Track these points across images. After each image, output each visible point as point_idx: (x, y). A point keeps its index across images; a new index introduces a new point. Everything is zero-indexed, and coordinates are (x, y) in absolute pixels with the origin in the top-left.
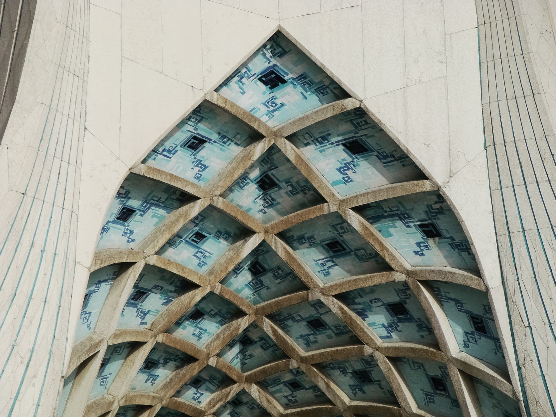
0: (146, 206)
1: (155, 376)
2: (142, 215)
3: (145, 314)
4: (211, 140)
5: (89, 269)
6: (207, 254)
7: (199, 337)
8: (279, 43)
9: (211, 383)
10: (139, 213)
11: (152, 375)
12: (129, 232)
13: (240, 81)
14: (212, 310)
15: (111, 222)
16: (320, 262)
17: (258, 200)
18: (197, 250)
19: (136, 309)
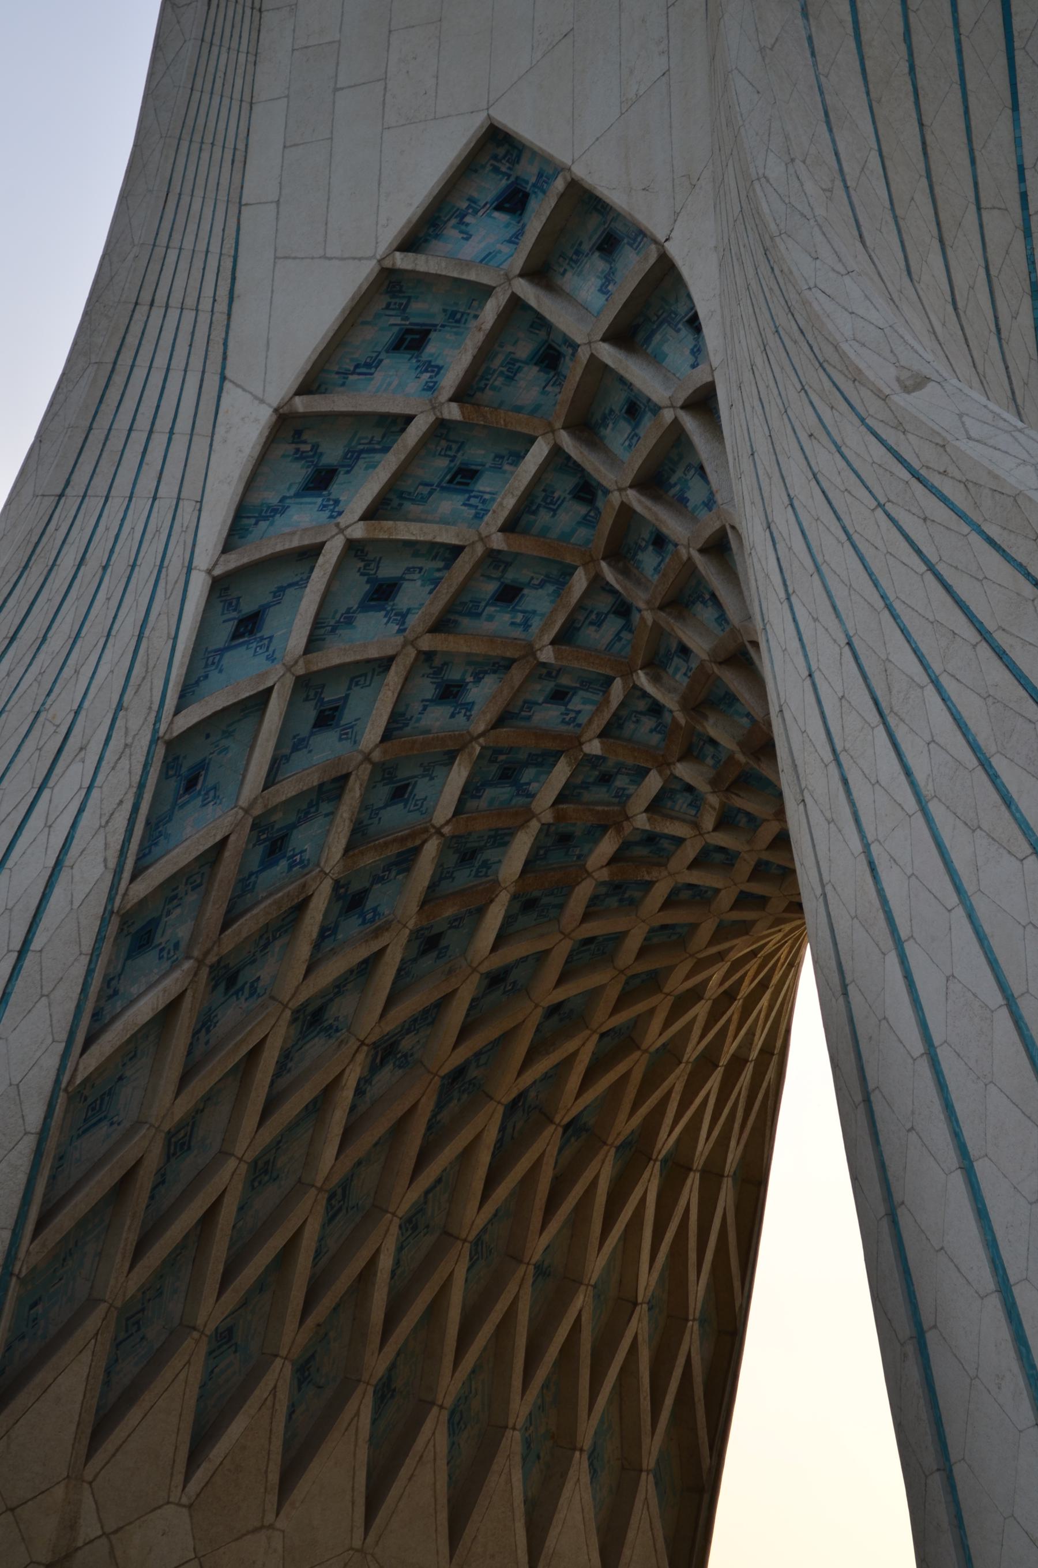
0: (352, 456)
1: (468, 704)
2: (348, 472)
3: (404, 616)
4: (436, 325)
5: (209, 572)
6: (487, 496)
7: (526, 625)
8: (496, 144)
9: (587, 690)
10: (342, 470)
11: (461, 704)
12: (331, 502)
13: (461, 222)
14: (532, 578)
15: (290, 497)
16: (627, 443)
17: (549, 389)
18: (467, 496)
19: (383, 613)
